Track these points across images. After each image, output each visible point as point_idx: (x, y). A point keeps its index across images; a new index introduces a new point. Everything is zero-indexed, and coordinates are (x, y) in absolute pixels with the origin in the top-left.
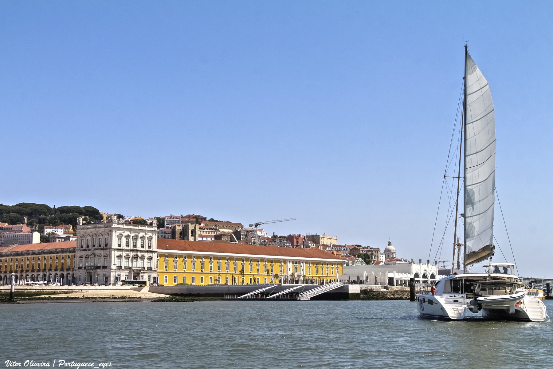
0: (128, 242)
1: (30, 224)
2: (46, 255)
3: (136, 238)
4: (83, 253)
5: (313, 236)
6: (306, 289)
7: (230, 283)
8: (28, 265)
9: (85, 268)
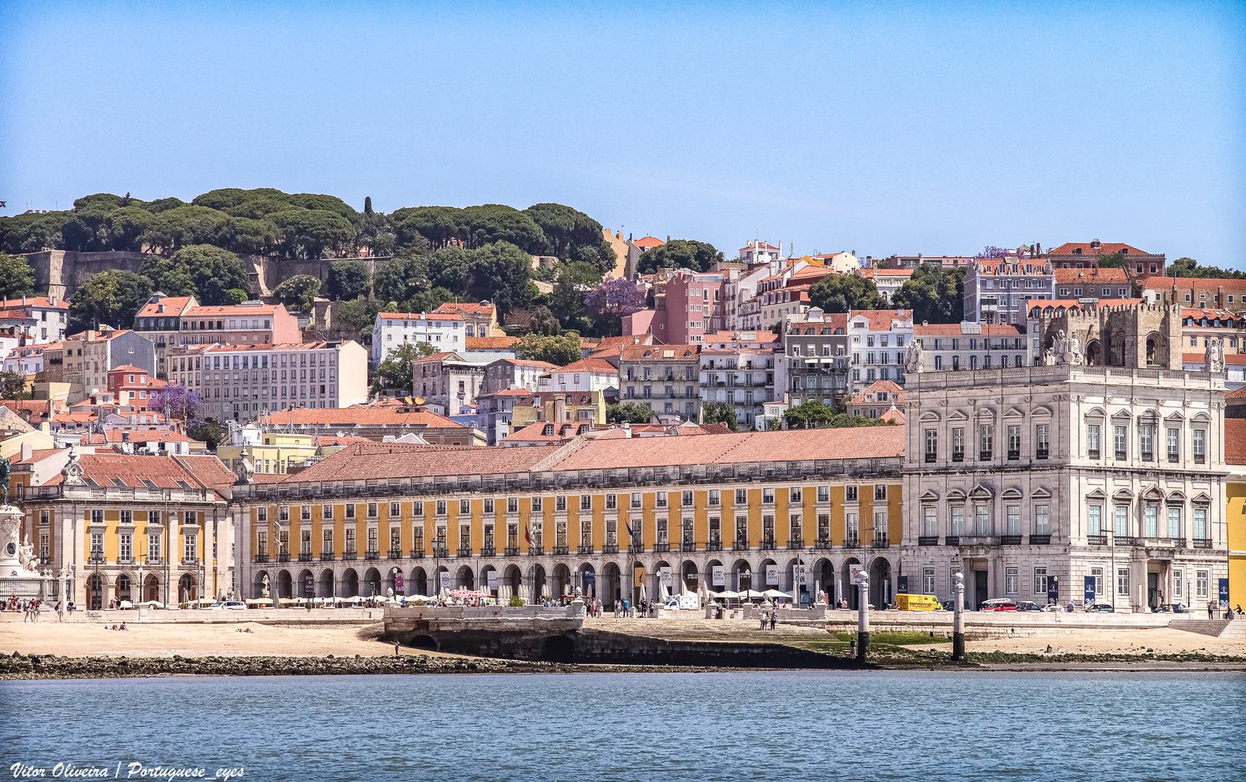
0: (1124, 439)
1: (294, 301)
2: (747, 487)
3: (1151, 422)
4: (939, 483)
8: (662, 523)
9: (952, 541)
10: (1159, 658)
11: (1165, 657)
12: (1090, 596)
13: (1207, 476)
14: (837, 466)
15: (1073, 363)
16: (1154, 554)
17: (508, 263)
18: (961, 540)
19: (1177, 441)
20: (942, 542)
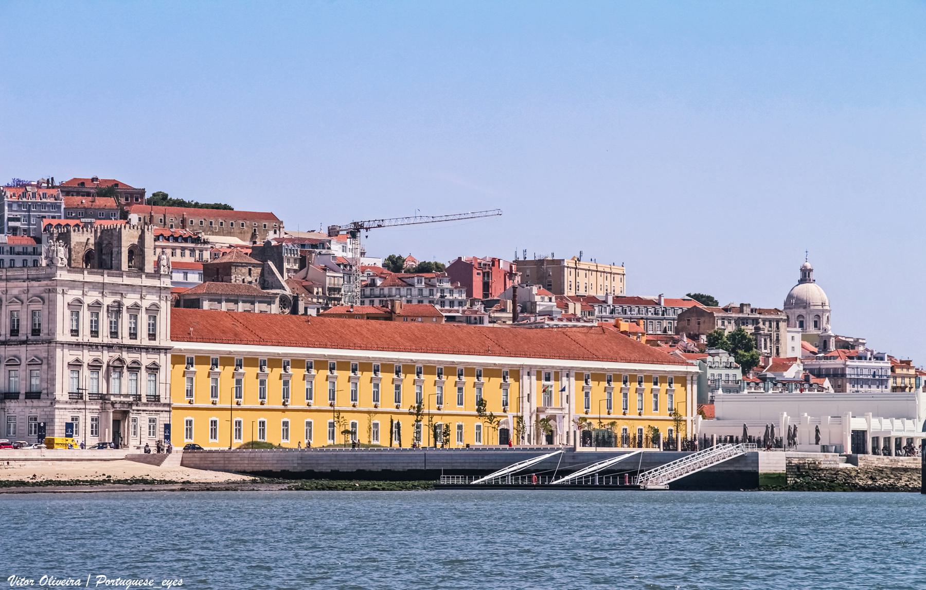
0: (97, 322)
3: (116, 310)
5: (541, 262)
6: (652, 462)
7: (383, 441)
10: (115, 482)
11: (119, 482)
13: (157, 350)
15: (59, 265)
16: (117, 406)
19: (136, 324)
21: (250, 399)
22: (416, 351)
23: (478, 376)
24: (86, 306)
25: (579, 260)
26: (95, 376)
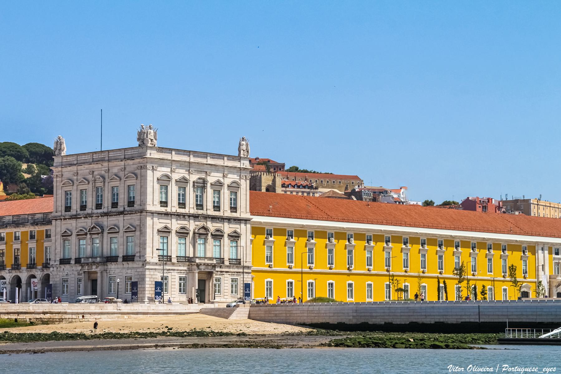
0: (184, 195)
3: (201, 185)
4: (72, 225)
5: (517, 201)
7: (431, 296)
12: (158, 294)
13: (238, 221)
14: (25, 219)
16: (202, 267)
17: (9, 165)
18: (82, 260)
19: (219, 198)
20: (73, 262)
21: (320, 266)
22: (454, 229)
23: (504, 250)
24: (173, 181)
25: (539, 200)
26: (183, 241)
